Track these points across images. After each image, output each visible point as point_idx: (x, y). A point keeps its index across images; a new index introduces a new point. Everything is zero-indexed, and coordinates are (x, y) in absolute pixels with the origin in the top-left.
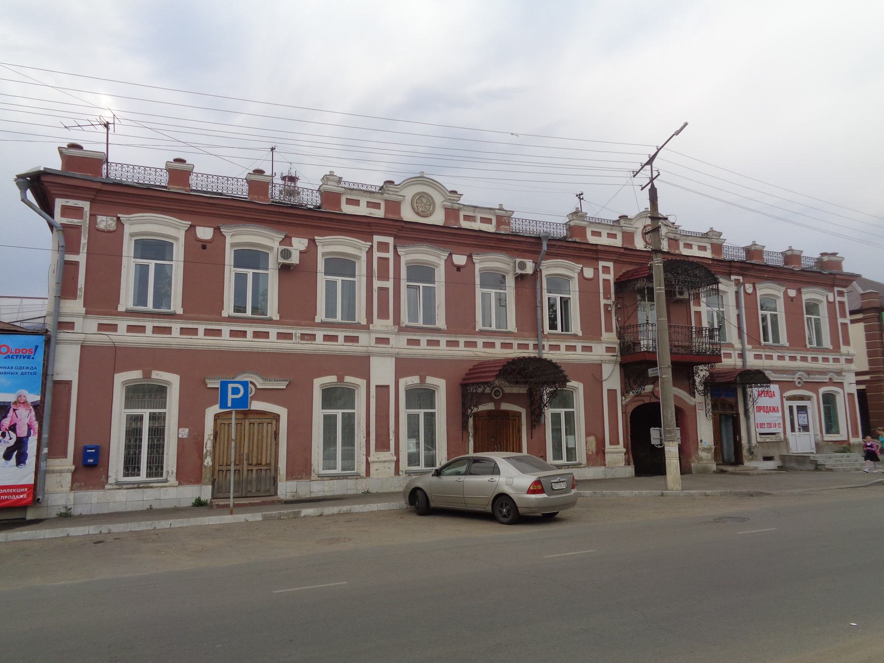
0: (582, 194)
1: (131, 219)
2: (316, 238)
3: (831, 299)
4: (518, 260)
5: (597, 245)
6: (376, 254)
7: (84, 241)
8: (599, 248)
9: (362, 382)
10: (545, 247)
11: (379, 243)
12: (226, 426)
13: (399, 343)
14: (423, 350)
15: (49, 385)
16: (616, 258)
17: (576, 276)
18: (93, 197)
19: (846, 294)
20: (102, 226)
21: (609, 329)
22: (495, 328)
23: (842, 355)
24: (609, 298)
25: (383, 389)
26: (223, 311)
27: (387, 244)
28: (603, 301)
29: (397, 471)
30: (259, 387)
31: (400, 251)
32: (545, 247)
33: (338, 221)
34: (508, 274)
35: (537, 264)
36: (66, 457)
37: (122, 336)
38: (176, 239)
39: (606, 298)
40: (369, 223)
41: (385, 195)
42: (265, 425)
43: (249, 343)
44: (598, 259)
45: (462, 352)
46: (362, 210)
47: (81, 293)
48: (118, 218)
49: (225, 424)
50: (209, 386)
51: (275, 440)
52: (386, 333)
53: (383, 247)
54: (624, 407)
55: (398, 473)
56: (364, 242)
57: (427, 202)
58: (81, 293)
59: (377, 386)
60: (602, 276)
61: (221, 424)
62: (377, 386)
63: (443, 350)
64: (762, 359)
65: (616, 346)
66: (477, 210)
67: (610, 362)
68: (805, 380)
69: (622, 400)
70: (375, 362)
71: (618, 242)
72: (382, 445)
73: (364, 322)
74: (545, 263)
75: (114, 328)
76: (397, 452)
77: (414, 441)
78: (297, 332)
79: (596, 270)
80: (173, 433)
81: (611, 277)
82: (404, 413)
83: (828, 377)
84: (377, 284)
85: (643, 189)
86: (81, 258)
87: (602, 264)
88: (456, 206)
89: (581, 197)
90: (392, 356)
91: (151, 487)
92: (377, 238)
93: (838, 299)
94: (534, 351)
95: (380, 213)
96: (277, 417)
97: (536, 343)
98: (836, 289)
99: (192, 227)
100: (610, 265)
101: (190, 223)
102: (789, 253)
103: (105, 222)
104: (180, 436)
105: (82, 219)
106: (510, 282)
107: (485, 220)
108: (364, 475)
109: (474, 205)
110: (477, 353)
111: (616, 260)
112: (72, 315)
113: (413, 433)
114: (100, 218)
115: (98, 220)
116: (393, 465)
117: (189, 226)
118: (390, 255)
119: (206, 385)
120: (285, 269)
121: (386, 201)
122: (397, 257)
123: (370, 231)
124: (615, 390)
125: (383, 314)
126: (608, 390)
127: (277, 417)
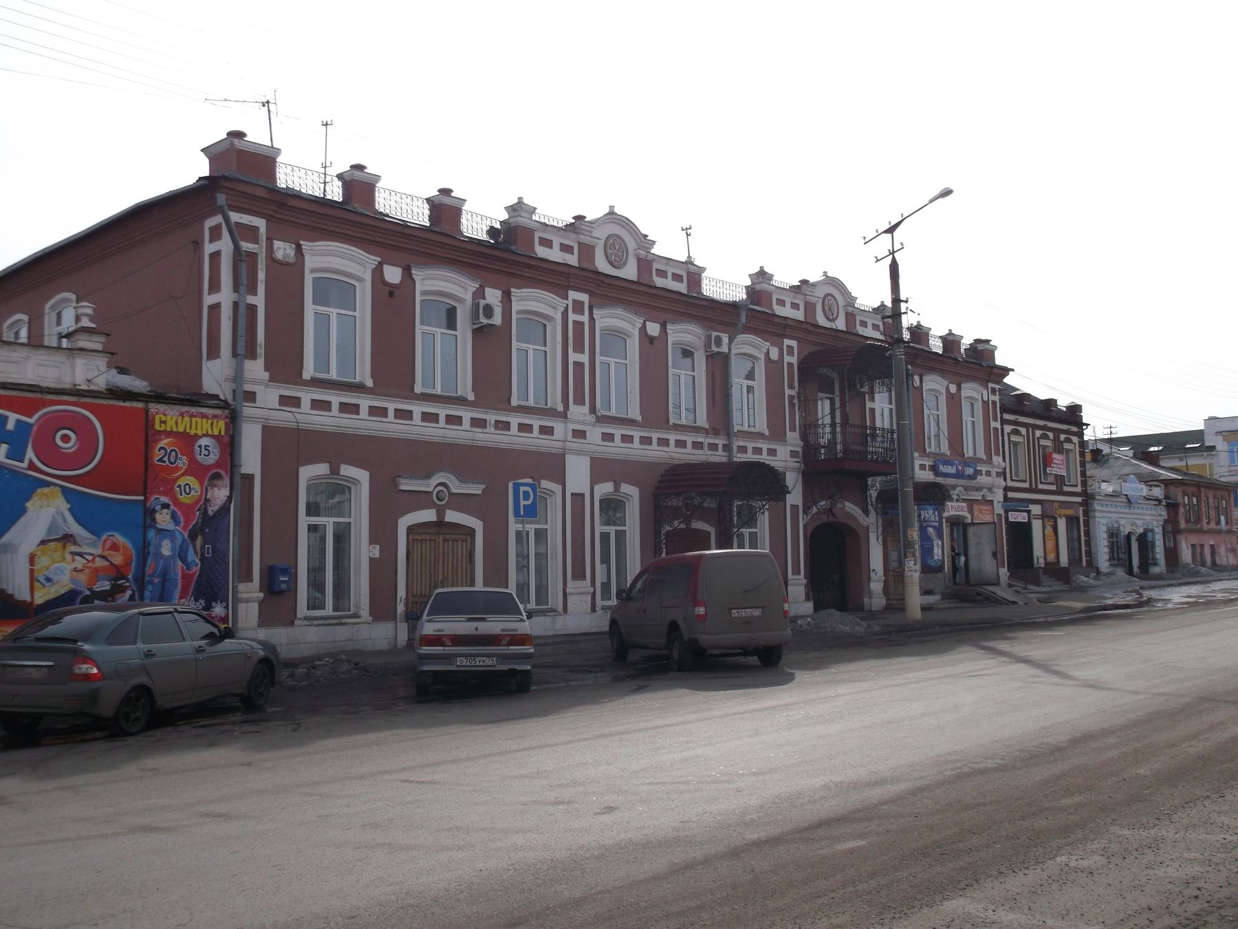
0: (690, 228)
1: (315, 248)
2: (512, 290)
3: (985, 399)
4: (714, 334)
5: (786, 318)
6: (572, 317)
7: (261, 276)
8: (789, 322)
9: (557, 488)
10: (743, 319)
11: (575, 301)
12: (419, 542)
13: (595, 434)
14: (617, 449)
15: (238, 479)
16: (800, 336)
17: (762, 357)
18: (272, 213)
19: (997, 392)
20: (279, 255)
21: (793, 429)
22: (614, 412)
23: (993, 467)
24: (794, 388)
25: (578, 497)
26: (415, 386)
27: (582, 303)
28: (788, 392)
29: (593, 609)
30: (454, 491)
31: (597, 313)
32: (743, 319)
33: (529, 266)
34: (697, 350)
35: (731, 341)
36: (251, 581)
37: (307, 417)
38: (360, 280)
39: (791, 387)
40: (569, 274)
41: (581, 236)
42: (460, 542)
43: (439, 432)
44: (783, 336)
45: (654, 453)
46: (554, 255)
47: (261, 350)
48: (299, 247)
49: (426, 540)
50: (402, 488)
51: (471, 562)
52: (583, 423)
53: (578, 308)
54: (805, 527)
55: (595, 608)
56: (560, 300)
57: (619, 248)
58: (261, 350)
59: (572, 494)
60: (787, 359)
61: (413, 540)
62: (572, 494)
63: (636, 451)
64: (925, 470)
65: (799, 449)
66: (671, 262)
67: (793, 470)
68: (962, 497)
69: (803, 518)
70: (570, 460)
71: (799, 315)
72: (579, 574)
73: (560, 408)
74: (741, 338)
75: (295, 402)
76: (593, 584)
77: (605, 566)
78: (492, 417)
79: (781, 350)
80: (363, 551)
81: (794, 360)
82: (599, 529)
83: (982, 493)
84: (573, 357)
85: (878, 261)
86: (259, 300)
87: (787, 342)
88: (650, 257)
89: (689, 231)
90: (585, 455)
91: (345, 624)
92: (573, 295)
93: (992, 398)
94: (724, 454)
95: (572, 260)
96: (471, 532)
97: (725, 442)
98: (990, 385)
99: (380, 264)
100: (794, 343)
101: (379, 259)
102: (950, 338)
103: (283, 250)
104: (372, 556)
105: (258, 244)
106: (700, 359)
107: (677, 278)
108: (560, 608)
109: (668, 257)
110: (672, 454)
111: (800, 338)
112: (254, 382)
113: (605, 559)
114: (277, 244)
115: (275, 247)
116: (589, 598)
117: (377, 263)
118: (585, 318)
119: (396, 485)
120: (480, 332)
121: (580, 244)
122: (592, 320)
123: (566, 284)
124: (798, 506)
125: (579, 401)
126: (791, 505)
127: (471, 532)
